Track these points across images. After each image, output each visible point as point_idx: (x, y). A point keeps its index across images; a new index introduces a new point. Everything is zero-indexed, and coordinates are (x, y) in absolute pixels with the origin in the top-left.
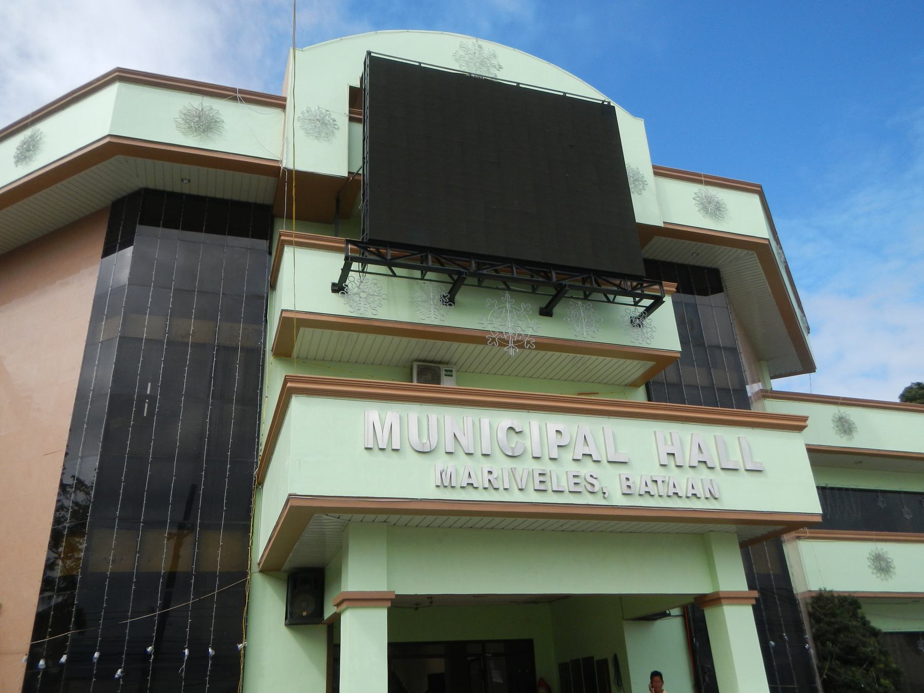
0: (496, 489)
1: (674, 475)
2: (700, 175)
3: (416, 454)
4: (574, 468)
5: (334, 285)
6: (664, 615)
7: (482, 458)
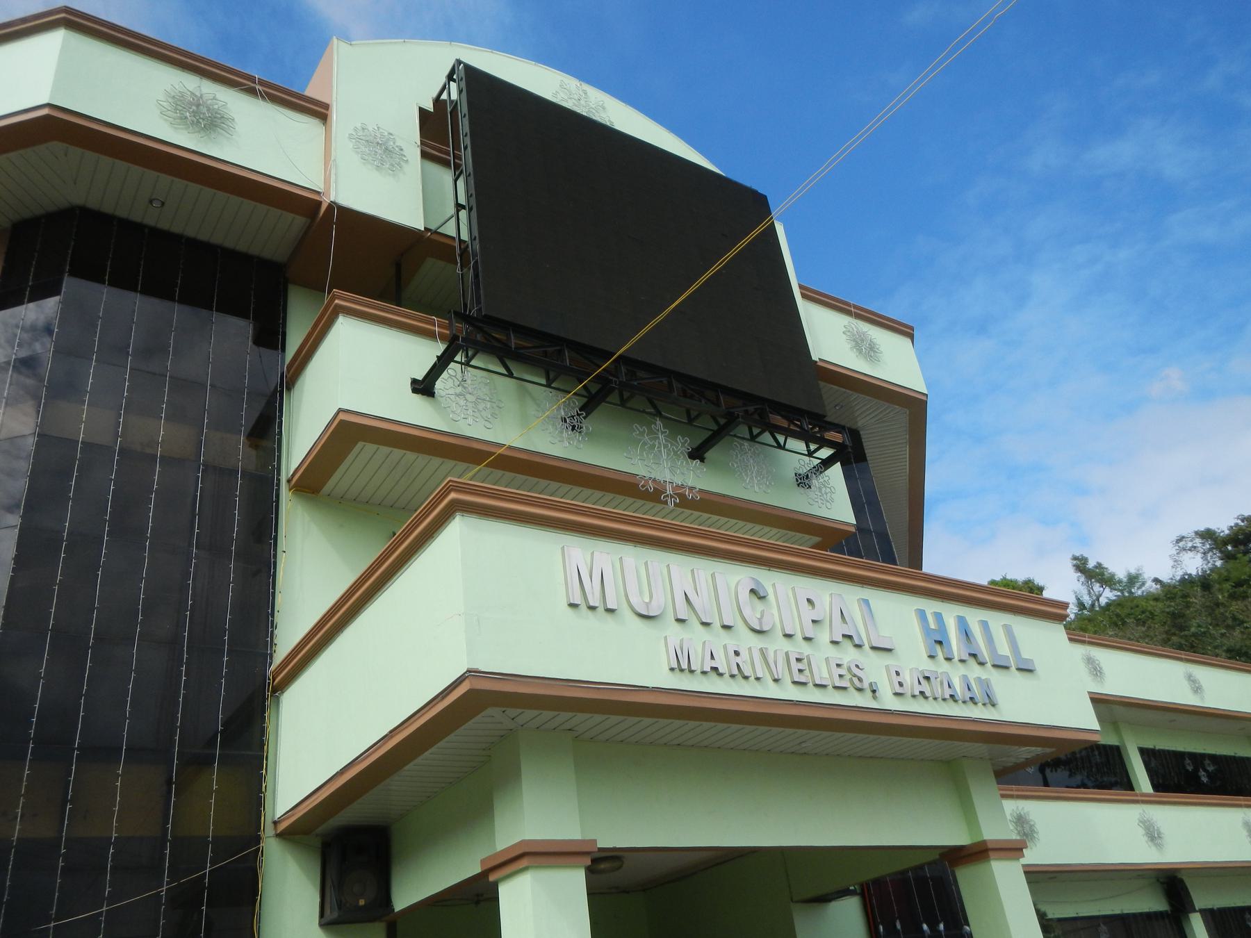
0: (746, 678)
1: (944, 667)
2: (848, 304)
3: (637, 620)
4: (832, 652)
5: (414, 381)
6: (844, 893)
7: (722, 631)
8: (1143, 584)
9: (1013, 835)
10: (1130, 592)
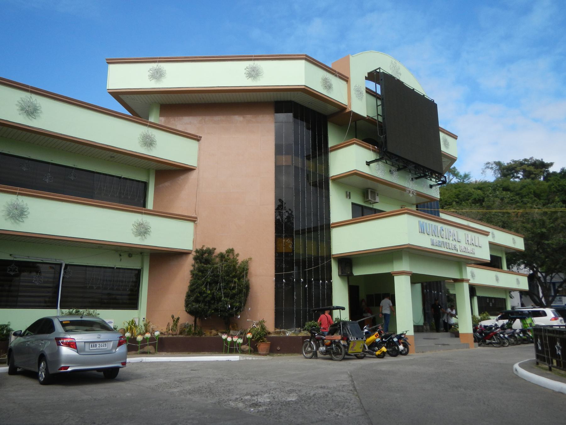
5: (367, 162)
8: (469, 179)
10: (464, 181)
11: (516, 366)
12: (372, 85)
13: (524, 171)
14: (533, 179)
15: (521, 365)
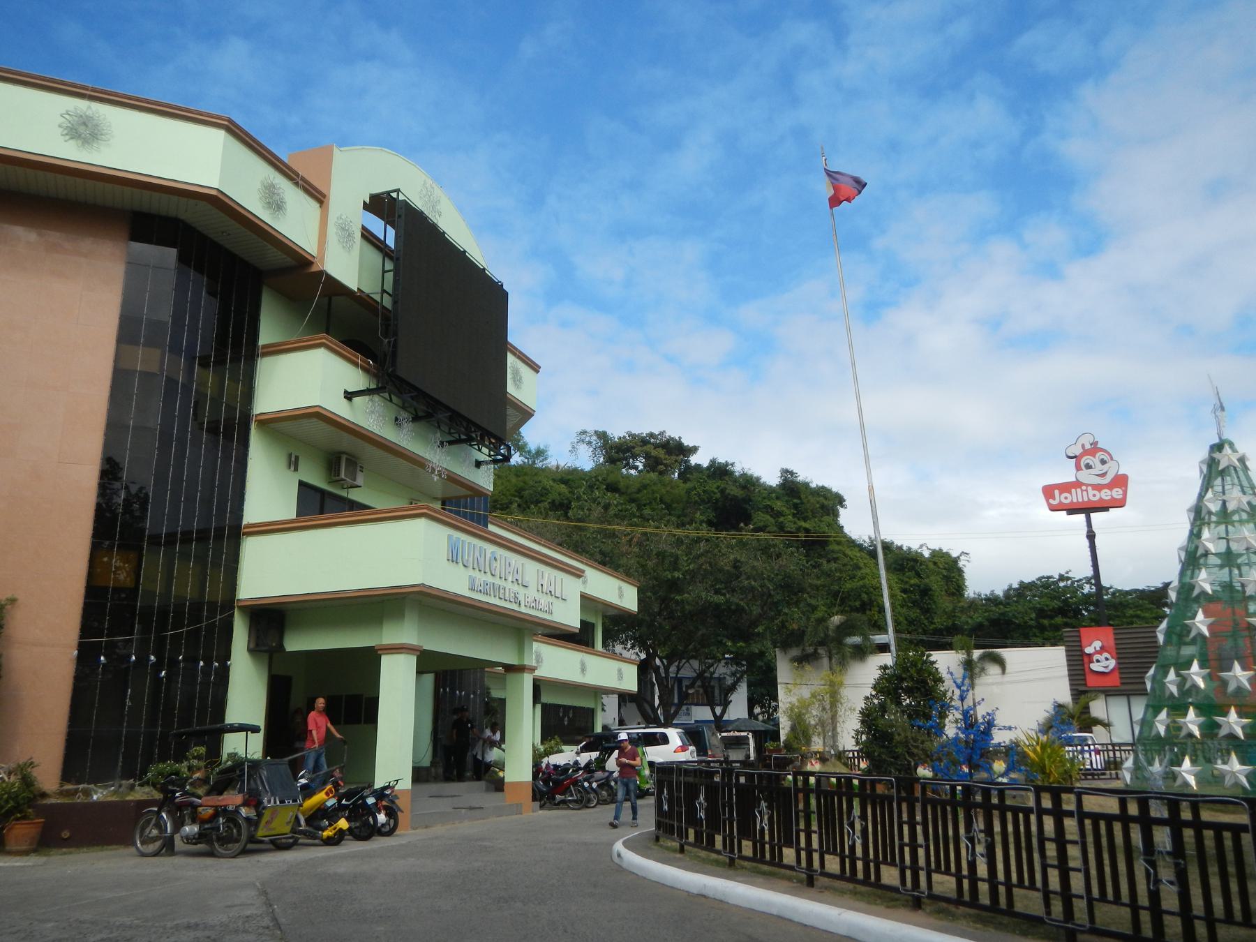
5: (346, 392)
9: (534, 664)
11: (619, 846)
12: (377, 226)
13: (647, 456)
14: (661, 473)
15: (626, 844)
